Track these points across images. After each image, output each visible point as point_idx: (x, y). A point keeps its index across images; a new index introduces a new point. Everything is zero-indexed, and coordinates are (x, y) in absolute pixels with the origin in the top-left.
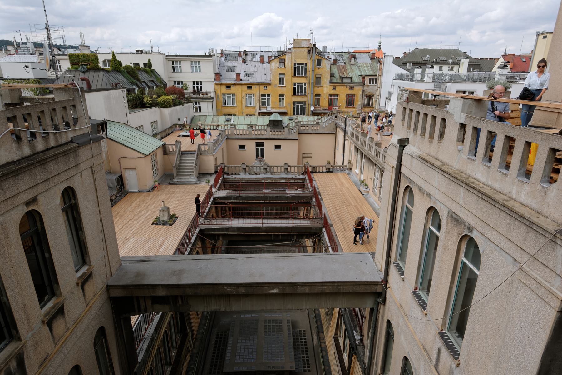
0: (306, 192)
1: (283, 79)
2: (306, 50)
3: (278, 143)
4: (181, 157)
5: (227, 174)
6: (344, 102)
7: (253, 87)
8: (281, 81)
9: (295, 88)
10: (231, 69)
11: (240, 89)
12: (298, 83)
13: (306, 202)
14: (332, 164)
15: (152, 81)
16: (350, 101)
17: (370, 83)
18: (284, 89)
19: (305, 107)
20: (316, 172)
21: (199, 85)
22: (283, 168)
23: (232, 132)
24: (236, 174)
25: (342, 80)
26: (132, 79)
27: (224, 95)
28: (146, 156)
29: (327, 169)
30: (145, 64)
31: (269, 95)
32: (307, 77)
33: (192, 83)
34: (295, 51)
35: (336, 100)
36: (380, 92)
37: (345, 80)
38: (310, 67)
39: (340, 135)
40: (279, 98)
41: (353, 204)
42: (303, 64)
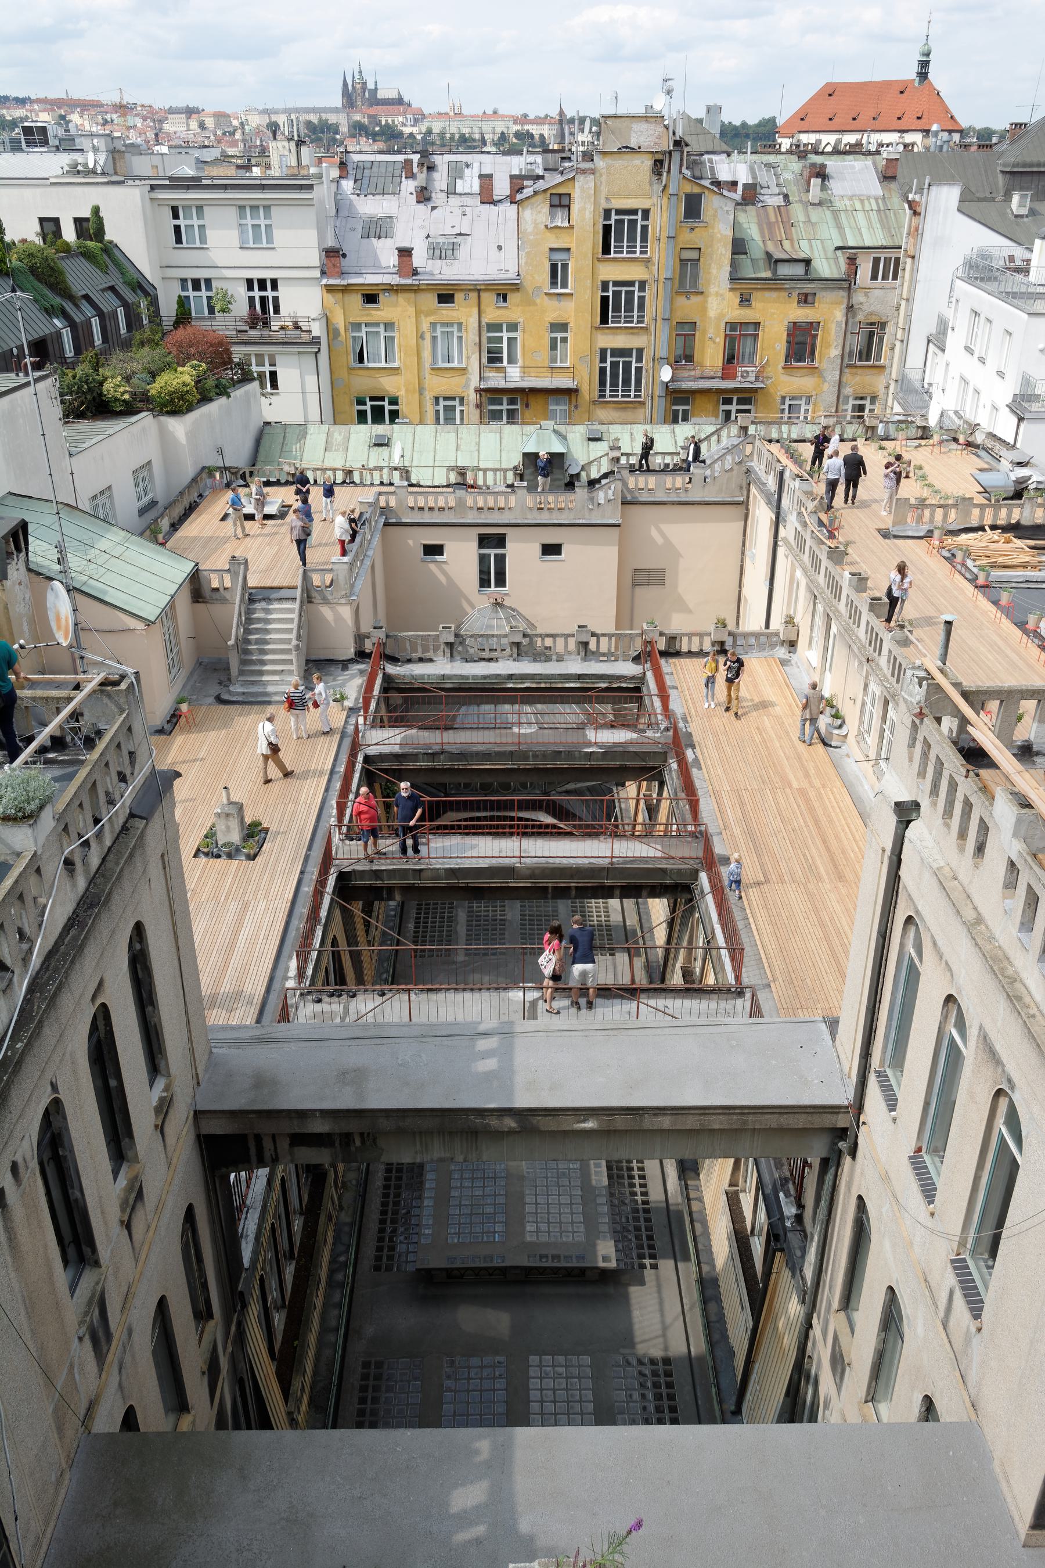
0: (649, 733)
1: (565, 267)
2: (648, 163)
3: (551, 537)
4: (249, 612)
5: (394, 660)
6: (781, 347)
7: (459, 297)
8: (557, 273)
9: (604, 300)
10: (378, 228)
11: (411, 310)
12: (616, 284)
13: (646, 767)
14: (731, 627)
15: (112, 289)
16: (801, 344)
17: (874, 277)
18: (569, 305)
19: (639, 370)
20: (678, 654)
21: (269, 293)
22: (572, 644)
23: (399, 502)
25: (774, 272)
26: (49, 294)
27: (357, 326)
28: (149, 623)
29: (713, 644)
30: (78, 221)
31: (513, 327)
32: (648, 261)
34: (608, 167)
35: (749, 341)
36: (909, 316)
37: (784, 270)
38: (660, 222)
39: (762, 514)
40: (547, 336)
41: (795, 785)
42: (634, 212)
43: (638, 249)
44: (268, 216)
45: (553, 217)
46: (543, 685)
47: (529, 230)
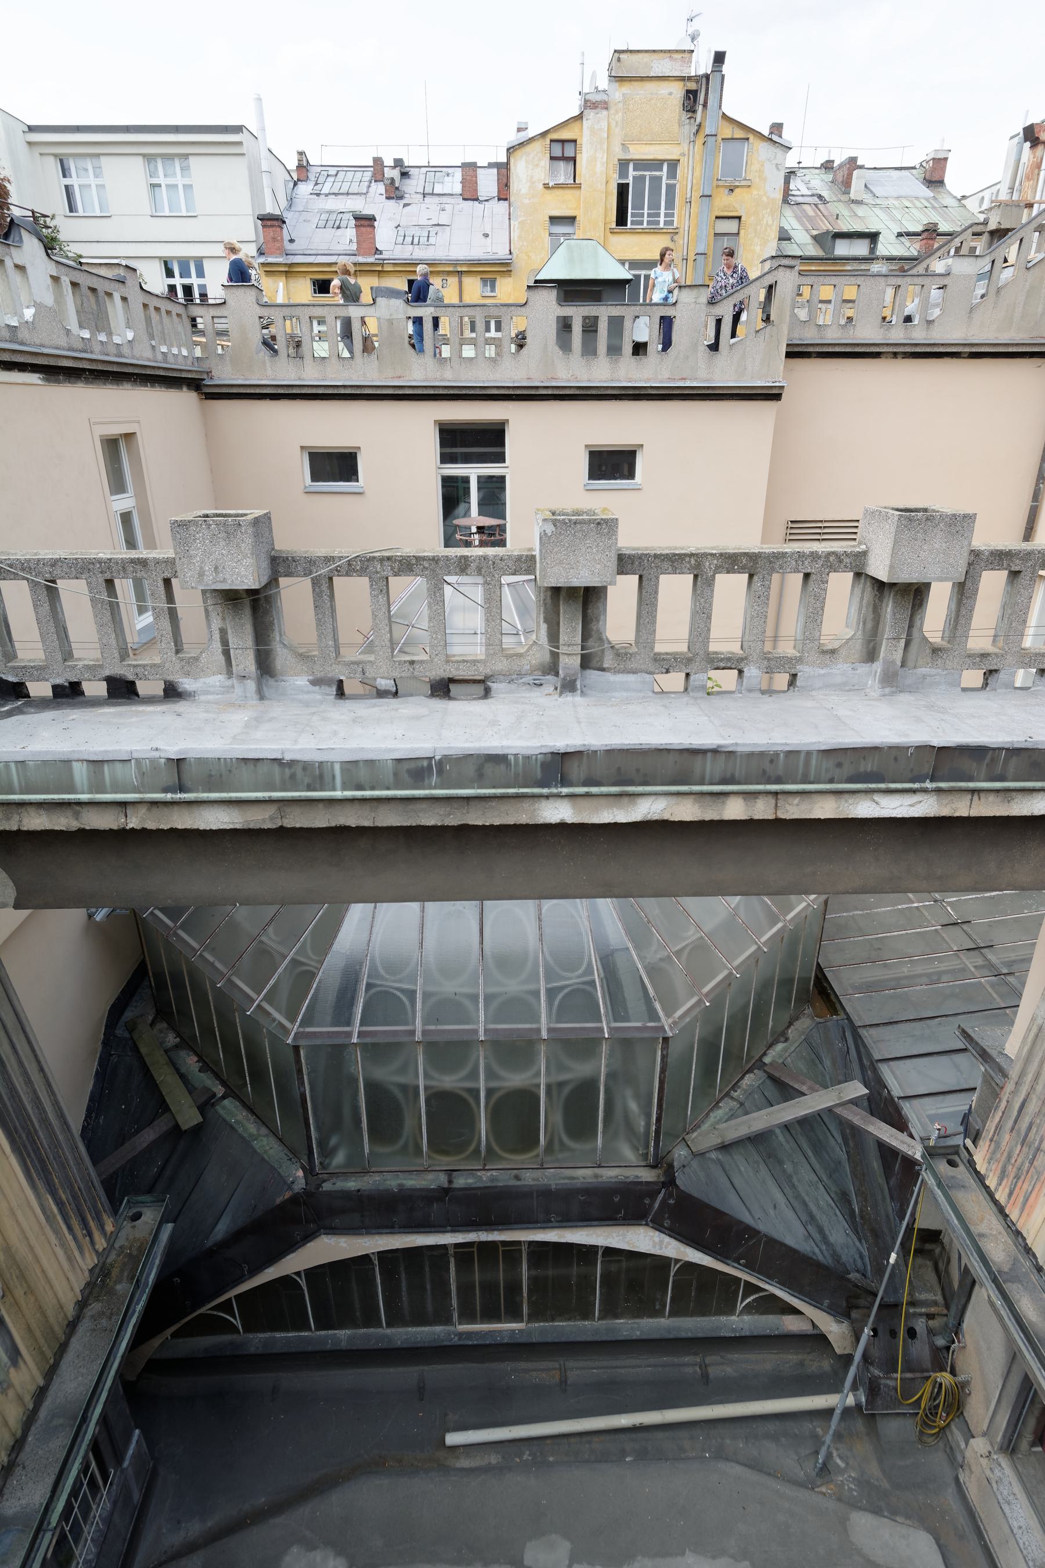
2: (677, 91)
21: (194, 281)
24: (122, 690)
33: (159, 269)
34: (625, 98)
37: (842, 248)
42: (656, 164)
43: (662, 219)
44: (185, 169)
45: (552, 171)
46: (734, 810)
47: (524, 191)
